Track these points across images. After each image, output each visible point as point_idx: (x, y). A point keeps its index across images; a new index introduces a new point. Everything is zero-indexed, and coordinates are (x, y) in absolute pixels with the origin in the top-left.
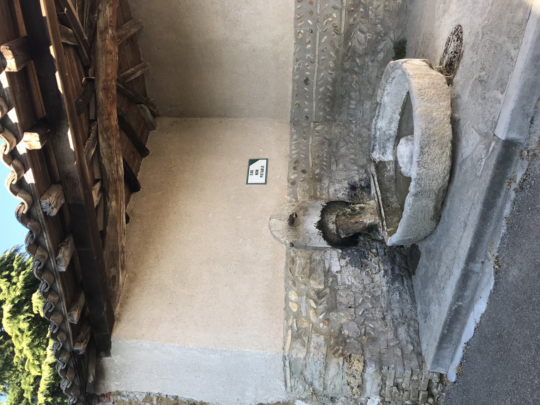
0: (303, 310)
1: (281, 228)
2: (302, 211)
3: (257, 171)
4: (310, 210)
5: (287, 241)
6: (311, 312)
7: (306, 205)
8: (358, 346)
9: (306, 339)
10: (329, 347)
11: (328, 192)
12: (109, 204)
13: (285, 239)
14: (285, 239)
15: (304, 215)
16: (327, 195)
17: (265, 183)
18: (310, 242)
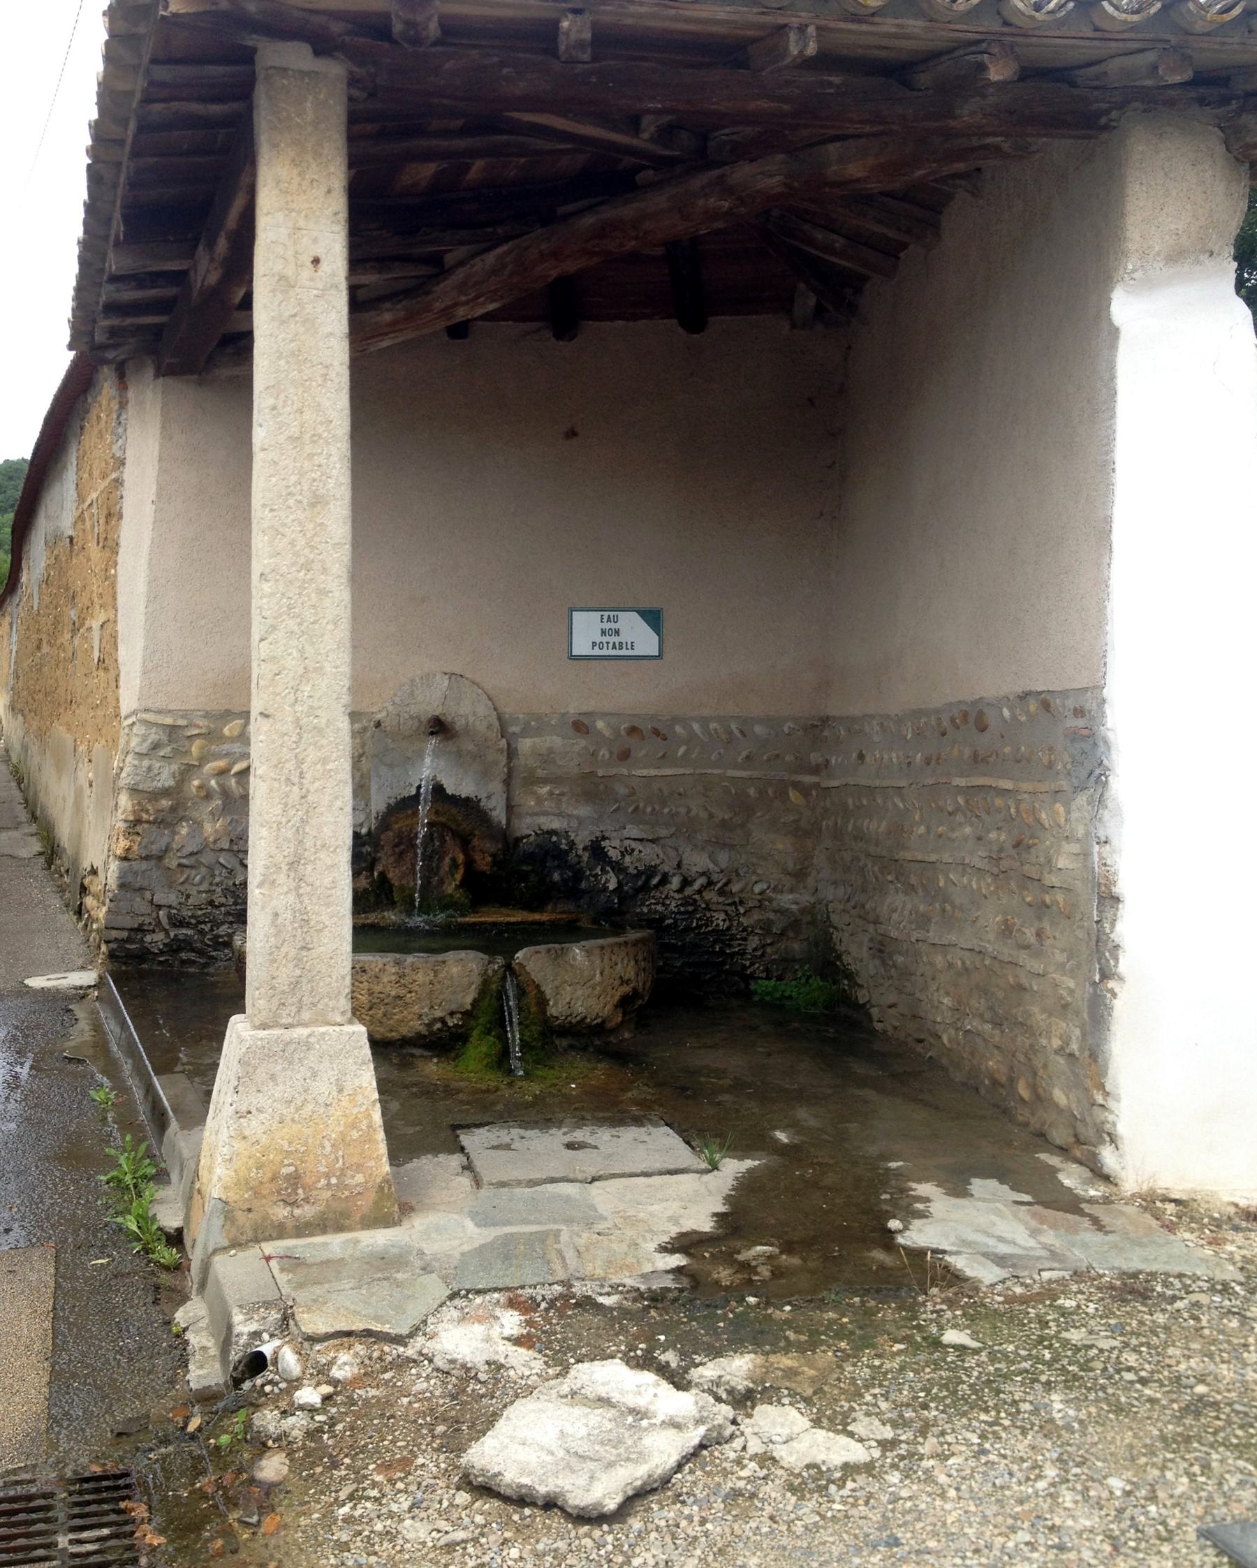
0: (226, 747)
3: (617, 632)
5: (384, 714)
6: (221, 764)
8: (155, 849)
9: (165, 751)
10: (156, 795)
11: (546, 814)
12: (388, 305)
13: (390, 708)
15: (459, 754)
16: (537, 809)
17: (572, 658)
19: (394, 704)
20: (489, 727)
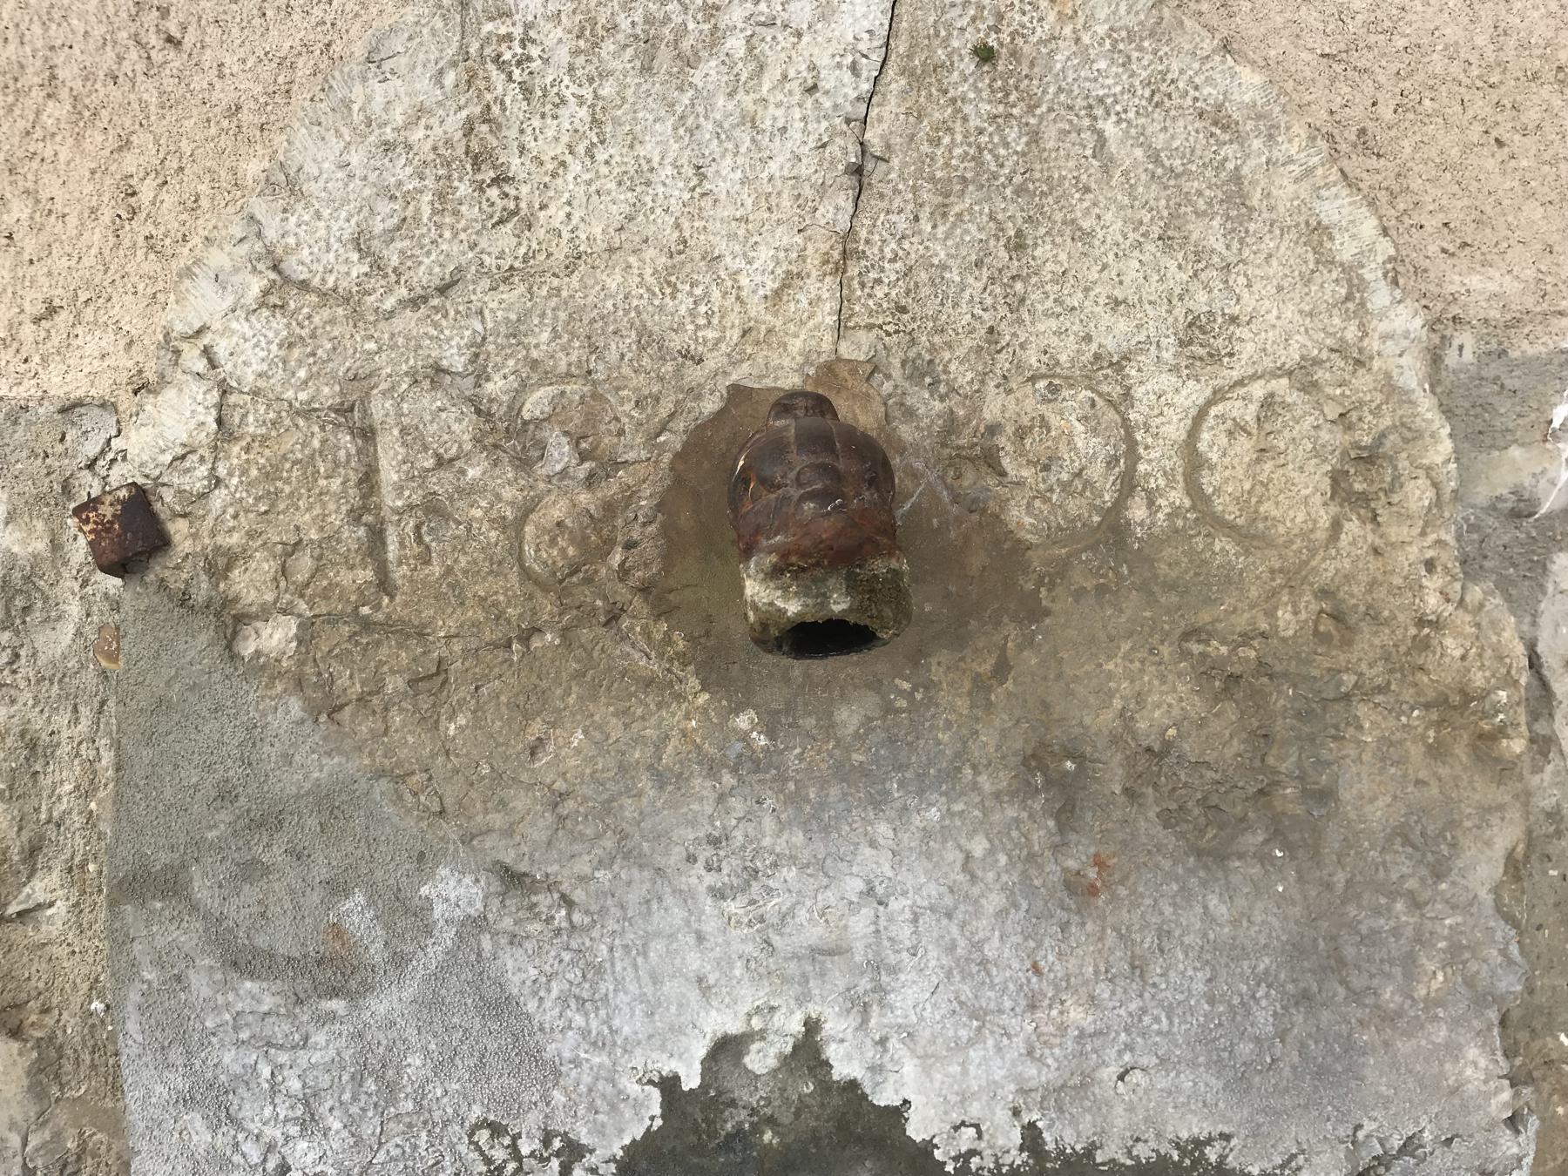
1: (578, 207)
2: (1166, 703)
4: (1247, 909)
7: (1369, 795)
13: (249, 349)
14: (249, 349)
15: (1054, 776)
18: (242, 961)
19: (283, 286)
20: (1361, 478)
